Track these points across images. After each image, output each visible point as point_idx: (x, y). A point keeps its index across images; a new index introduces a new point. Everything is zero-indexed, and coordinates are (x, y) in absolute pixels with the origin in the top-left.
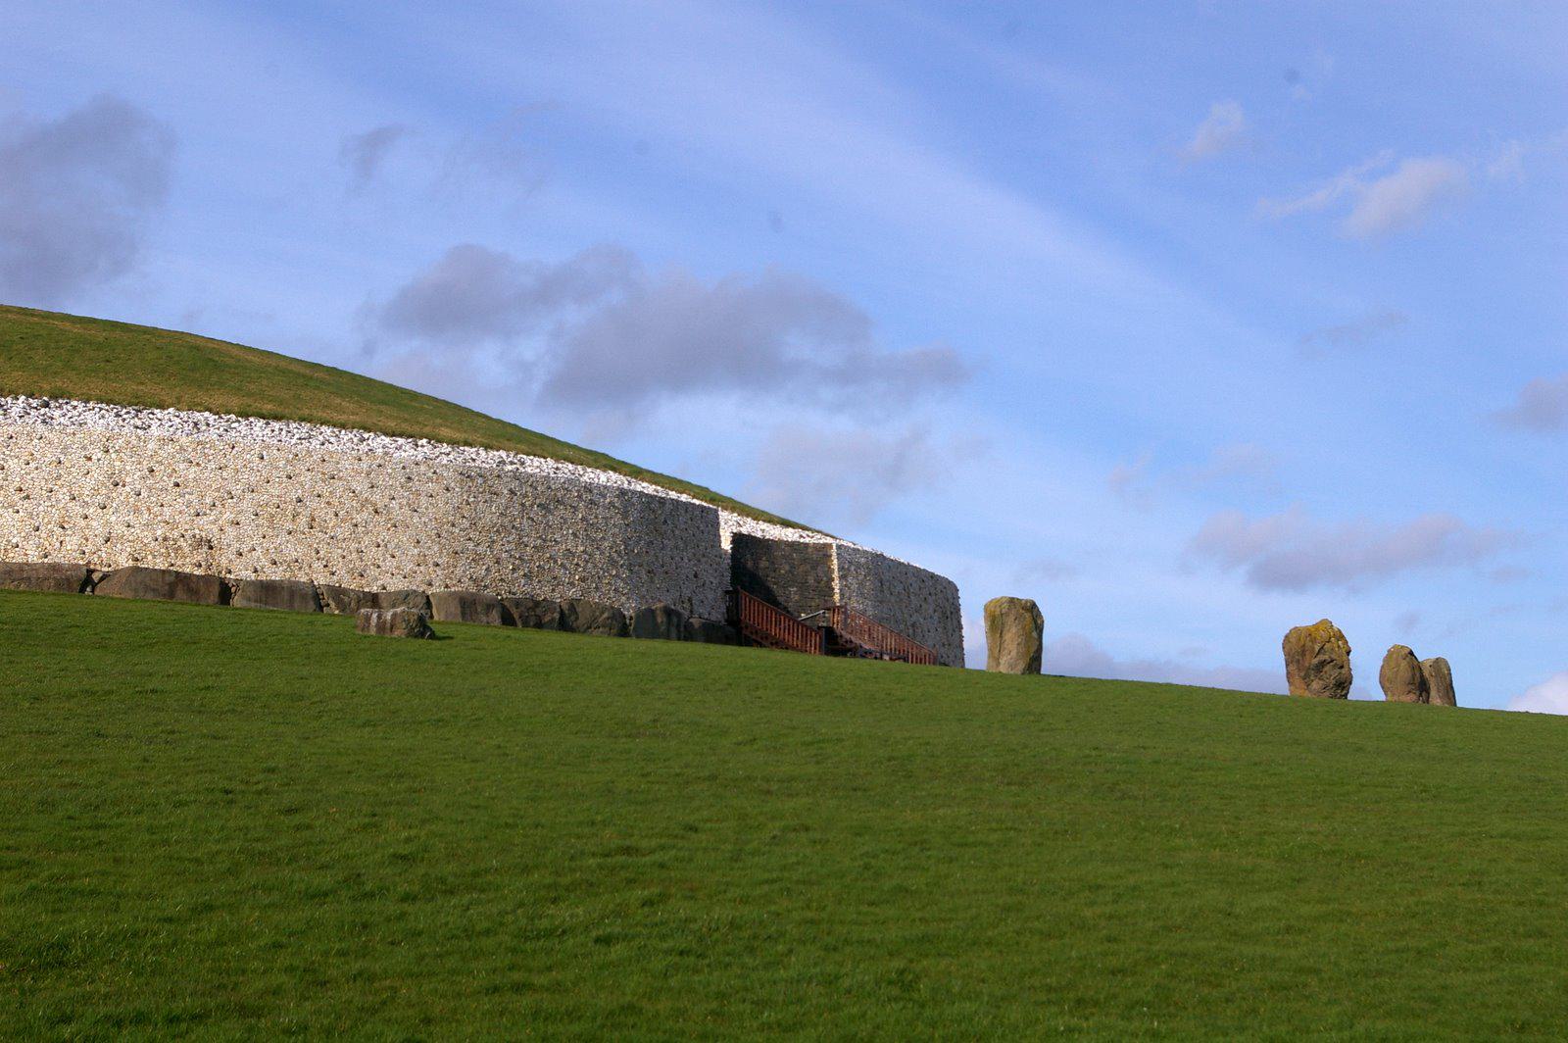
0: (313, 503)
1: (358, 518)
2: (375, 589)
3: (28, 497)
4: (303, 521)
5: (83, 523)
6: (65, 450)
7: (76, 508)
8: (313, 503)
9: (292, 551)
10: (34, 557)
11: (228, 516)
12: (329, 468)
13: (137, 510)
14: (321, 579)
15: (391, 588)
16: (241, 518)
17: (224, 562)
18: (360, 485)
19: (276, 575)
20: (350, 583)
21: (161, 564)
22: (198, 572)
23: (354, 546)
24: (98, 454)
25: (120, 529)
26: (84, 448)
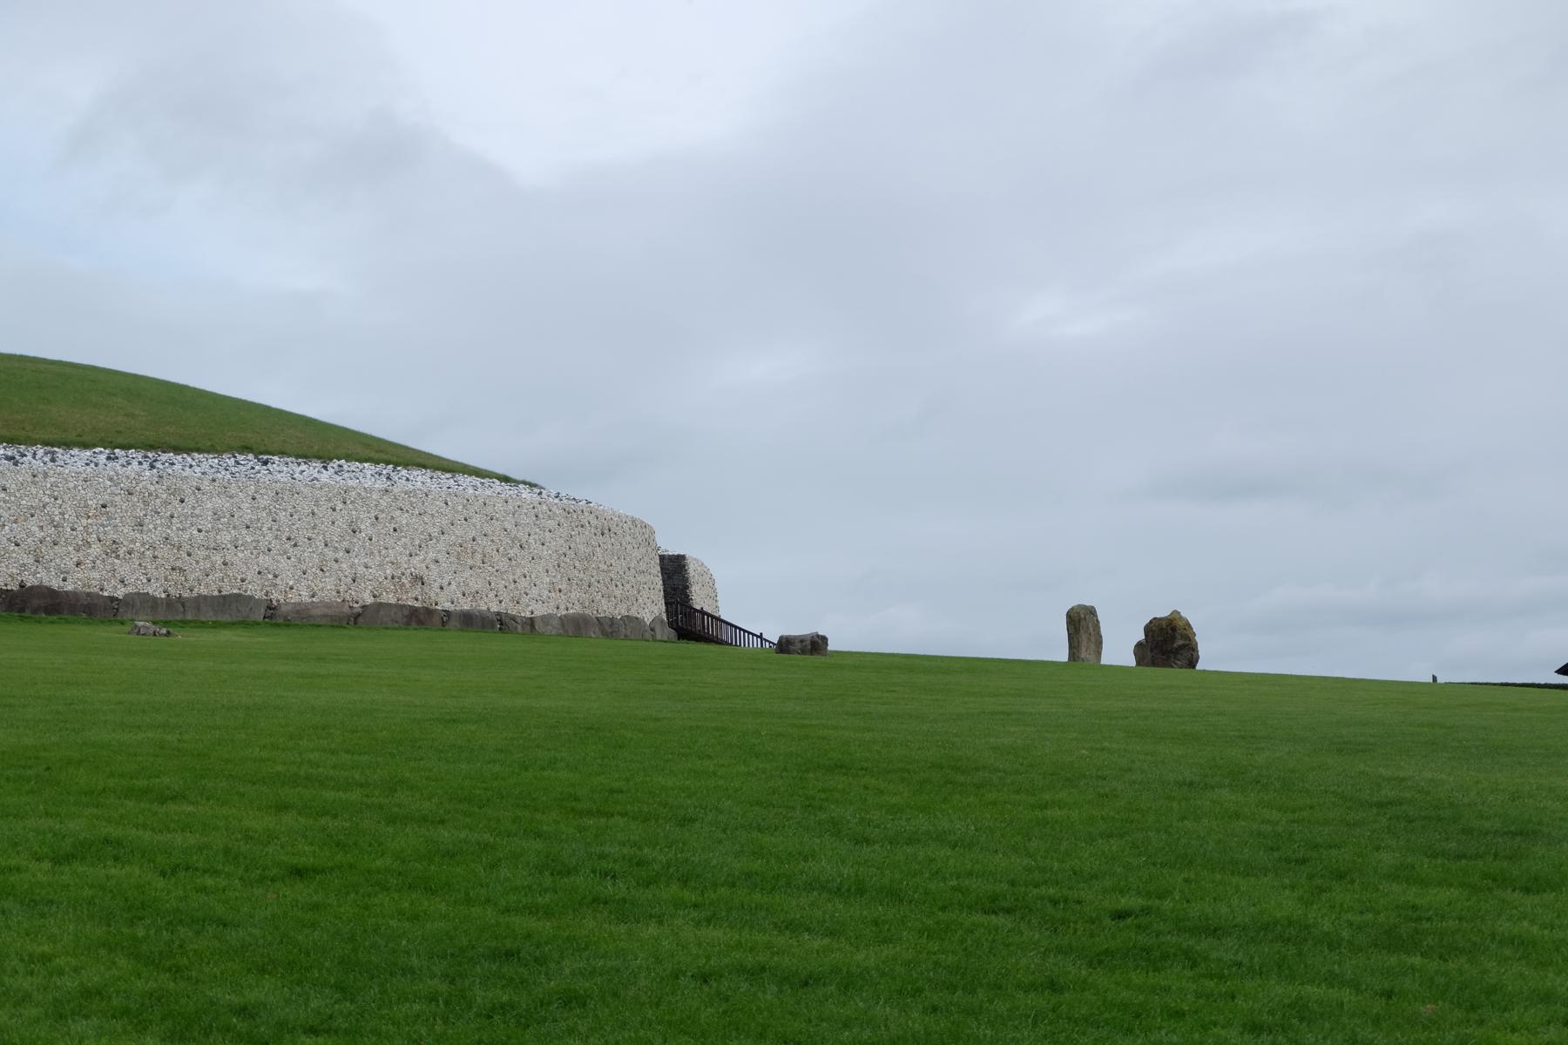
0: (481, 541)
1: (512, 554)
2: (528, 615)
4: (479, 556)
5: (336, 566)
6: (317, 504)
7: (330, 553)
8: (481, 541)
9: (475, 585)
10: (306, 598)
11: (431, 555)
12: (489, 510)
14: (494, 609)
15: (537, 613)
16: (440, 557)
19: (465, 605)
21: (389, 598)
22: (417, 605)
24: (340, 506)
25: (361, 570)
26: (329, 500)
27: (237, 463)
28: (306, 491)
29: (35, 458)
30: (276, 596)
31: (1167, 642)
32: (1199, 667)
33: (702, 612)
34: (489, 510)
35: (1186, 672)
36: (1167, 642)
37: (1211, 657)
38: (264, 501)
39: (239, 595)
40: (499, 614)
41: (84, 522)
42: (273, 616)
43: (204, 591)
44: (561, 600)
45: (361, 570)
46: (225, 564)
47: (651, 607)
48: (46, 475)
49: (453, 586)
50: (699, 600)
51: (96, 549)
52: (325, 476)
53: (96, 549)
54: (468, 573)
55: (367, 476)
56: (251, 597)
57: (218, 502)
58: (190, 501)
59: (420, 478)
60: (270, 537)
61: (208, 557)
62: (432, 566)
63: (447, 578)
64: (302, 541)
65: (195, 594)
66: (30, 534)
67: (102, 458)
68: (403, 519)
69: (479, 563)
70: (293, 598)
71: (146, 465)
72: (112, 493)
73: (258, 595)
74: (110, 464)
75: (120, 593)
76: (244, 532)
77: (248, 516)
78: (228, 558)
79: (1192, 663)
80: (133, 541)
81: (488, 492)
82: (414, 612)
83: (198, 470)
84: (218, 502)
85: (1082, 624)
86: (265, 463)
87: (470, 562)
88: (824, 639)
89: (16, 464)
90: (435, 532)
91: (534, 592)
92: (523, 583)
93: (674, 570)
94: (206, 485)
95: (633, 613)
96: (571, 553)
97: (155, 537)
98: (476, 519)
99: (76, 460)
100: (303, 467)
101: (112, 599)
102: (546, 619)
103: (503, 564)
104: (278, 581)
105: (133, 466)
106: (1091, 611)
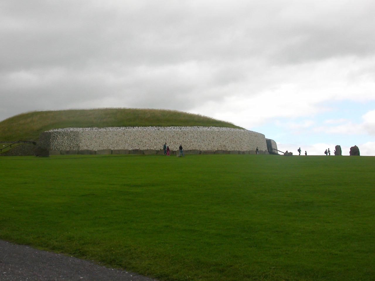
1: (240, 141)
2: (243, 151)
3: (204, 141)
4: (234, 141)
5: (211, 144)
7: (210, 142)
9: (234, 146)
10: (206, 149)
11: (227, 142)
12: (236, 134)
13: (217, 142)
14: (237, 150)
15: (245, 150)
16: (228, 142)
17: (227, 149)
18: (239, 136)
19: (233, 150)
20: (241, 150)
21: (220, 149)
22: (225, 150)
23: (240, 145)
27: (194, 128)
28: (205, 132)
29: (162, 129)
30: (201, 149)
31: (355, 151)
32: (361, 155)
33: (274, 149)
34: (236, 134)
35: (358, 156)
36: (355, 151)
37: (362, 153)
38: (198, 134)
39: (195, 150)
40: (238, 151)
41: (170, 139)
42: (200, 152)
43: (190, 149)
44: (249, 148)
45: (215, 145)
46: (193, 144)
47: (264, 148)
48: (164, 131)
49: (230, 147)
50: (273, 147)
51: (172, 143)
52: (208, 129)
53: (172, 143)
54: (233, 144)
55: (216, 129)
56: (197, 150)
57: (192, 135)
58: (187, 135)
59: (224, 129)
60: (200, 140)
61: (190, 144)
62: (227, 143)
63: (230, 145)
64: (205, 140)
65: (188, 150)
66: (162, 141)
67: (172, 128)
68: (222, 136)
69: (235, 143)
70: (204, 150)
71: (179, 129)
72: (174, 134)
73: (198, 149)
74: (174, 129)
75: (176, 150)
76: (196, 139)
77: (196, 137)
78: (193, 143)
79: (359, 155)
80: (178, 142)
81: (236, 131)
82: (224, 151)
83: (188, 129)
84: (192, 135)
85: (338, 149)
86: (198, 128)
87: (233, 142)
88: (292, 153)
89: (159, 130)
90: (227, 138)
91: (244, 147)
92: (242, 145)
93: (269, 143)
94: (189, 132)
95: (261, 150)
96: (250, 140)
97: (181, 141)
98: (234, 135)
99: (168, 129)
100: (205, 128)
101: (175, 151)
102: (246, 151)
103: (239, 143)
104: (201, 147)
105: (177, 129)
106: (340, 146)
